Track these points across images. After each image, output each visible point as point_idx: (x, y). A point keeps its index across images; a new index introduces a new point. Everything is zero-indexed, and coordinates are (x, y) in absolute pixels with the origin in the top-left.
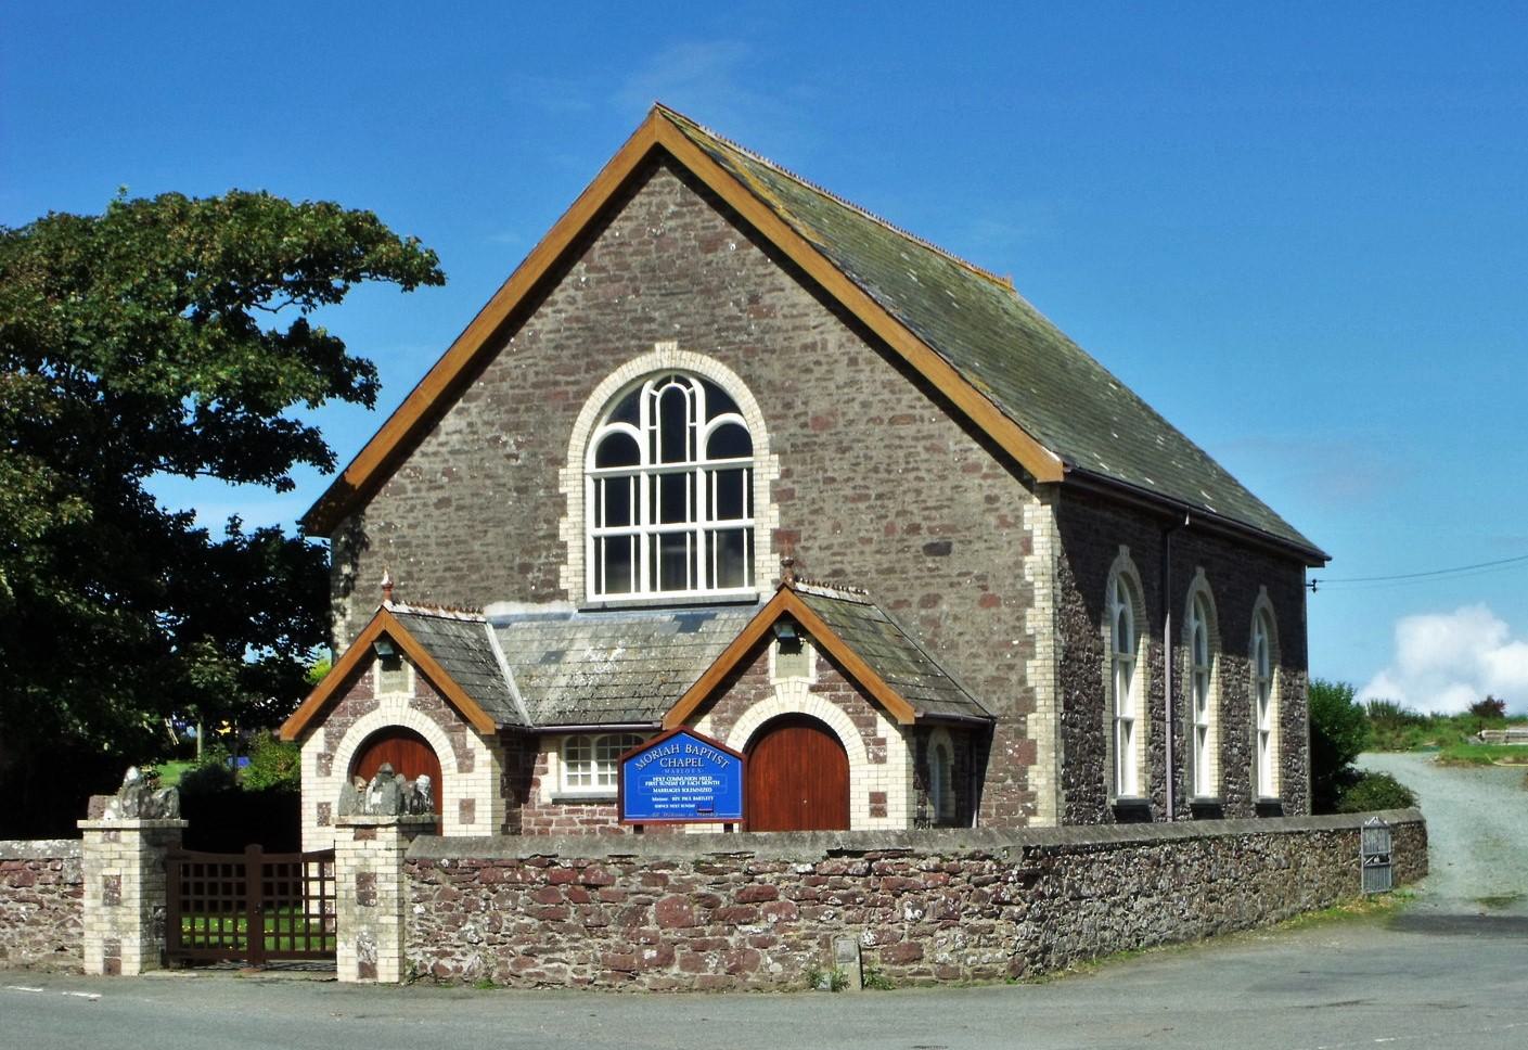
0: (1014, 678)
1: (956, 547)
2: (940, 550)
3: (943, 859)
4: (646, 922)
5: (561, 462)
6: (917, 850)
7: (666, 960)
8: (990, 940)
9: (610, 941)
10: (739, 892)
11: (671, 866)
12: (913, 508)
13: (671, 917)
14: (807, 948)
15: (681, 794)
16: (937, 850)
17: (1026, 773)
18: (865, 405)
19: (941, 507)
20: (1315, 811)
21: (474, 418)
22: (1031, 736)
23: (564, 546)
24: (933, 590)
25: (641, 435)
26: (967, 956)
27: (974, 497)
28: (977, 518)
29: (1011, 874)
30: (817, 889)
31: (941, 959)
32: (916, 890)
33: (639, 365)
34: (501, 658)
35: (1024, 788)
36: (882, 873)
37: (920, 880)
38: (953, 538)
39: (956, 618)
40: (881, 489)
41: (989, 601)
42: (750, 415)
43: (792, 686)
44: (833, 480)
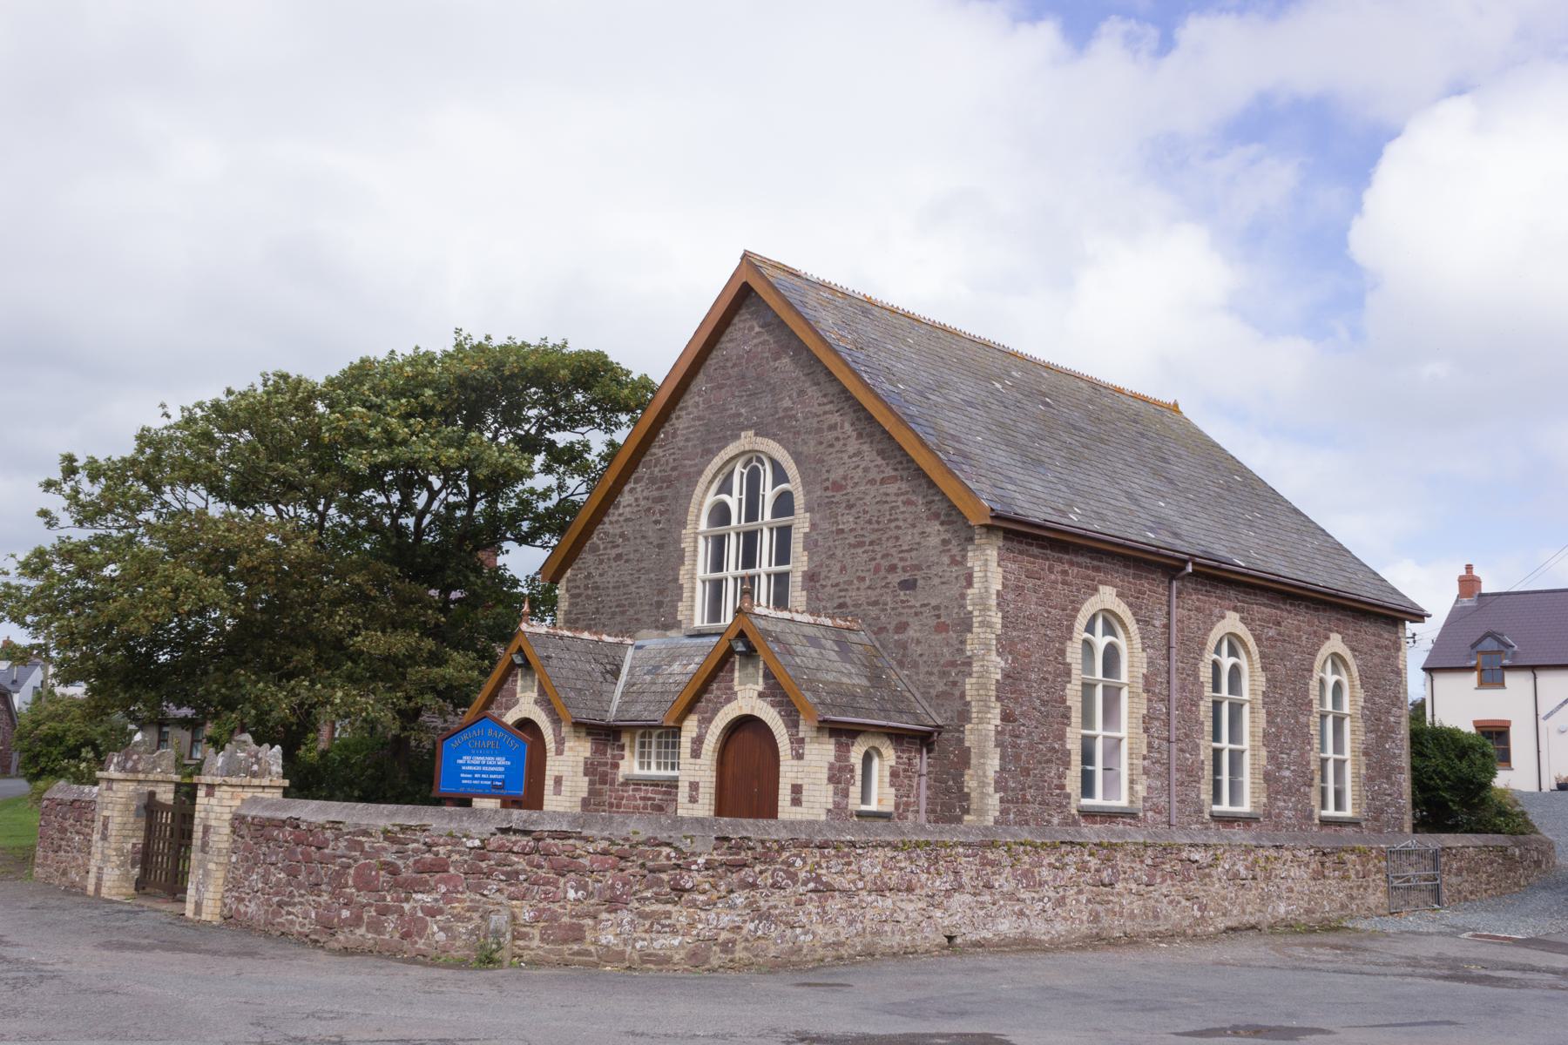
0: (957, 693)
1: (920, 583)
2: (909, 585)
3: (613, 843)
4: (346, 886)
5: (683, 524)
6: (585, 833)
7: (357, 921)
8: (663, 926)
9: (321, 899)
10: (416, 862)
11: (366, 833)
12: (893, 551)
13: (365, 884)
14: (470, 919)
15: (481, 772)
16: (606, 834)
17: (962, 775)
18: (866, 470)
19: (911, 550)
20: (1421, 826)
21: (638, 495)
22: (967, 744)
23: (681, 587)
24: (904, 619)
25: (732, 502)
26: (635, 940)
27: (934, 541)
28: (935, 559)
29: (695, 862)
30: (484, 865)
31: (604, 942)
32: (579, 870)
33: (731, 449)
34: (625, 670)
35: (961, 789)
36: (547, 854)
37: (585, 861)
38: (919, 575)
39: (918, 642)
40: (874, 537)
41: (941, 628)
42: (795, 485)
43: (747, 696)
44: (842, 531)
